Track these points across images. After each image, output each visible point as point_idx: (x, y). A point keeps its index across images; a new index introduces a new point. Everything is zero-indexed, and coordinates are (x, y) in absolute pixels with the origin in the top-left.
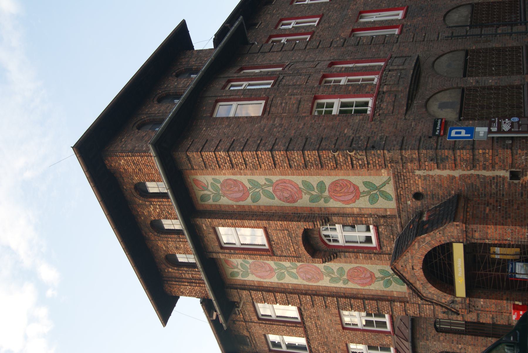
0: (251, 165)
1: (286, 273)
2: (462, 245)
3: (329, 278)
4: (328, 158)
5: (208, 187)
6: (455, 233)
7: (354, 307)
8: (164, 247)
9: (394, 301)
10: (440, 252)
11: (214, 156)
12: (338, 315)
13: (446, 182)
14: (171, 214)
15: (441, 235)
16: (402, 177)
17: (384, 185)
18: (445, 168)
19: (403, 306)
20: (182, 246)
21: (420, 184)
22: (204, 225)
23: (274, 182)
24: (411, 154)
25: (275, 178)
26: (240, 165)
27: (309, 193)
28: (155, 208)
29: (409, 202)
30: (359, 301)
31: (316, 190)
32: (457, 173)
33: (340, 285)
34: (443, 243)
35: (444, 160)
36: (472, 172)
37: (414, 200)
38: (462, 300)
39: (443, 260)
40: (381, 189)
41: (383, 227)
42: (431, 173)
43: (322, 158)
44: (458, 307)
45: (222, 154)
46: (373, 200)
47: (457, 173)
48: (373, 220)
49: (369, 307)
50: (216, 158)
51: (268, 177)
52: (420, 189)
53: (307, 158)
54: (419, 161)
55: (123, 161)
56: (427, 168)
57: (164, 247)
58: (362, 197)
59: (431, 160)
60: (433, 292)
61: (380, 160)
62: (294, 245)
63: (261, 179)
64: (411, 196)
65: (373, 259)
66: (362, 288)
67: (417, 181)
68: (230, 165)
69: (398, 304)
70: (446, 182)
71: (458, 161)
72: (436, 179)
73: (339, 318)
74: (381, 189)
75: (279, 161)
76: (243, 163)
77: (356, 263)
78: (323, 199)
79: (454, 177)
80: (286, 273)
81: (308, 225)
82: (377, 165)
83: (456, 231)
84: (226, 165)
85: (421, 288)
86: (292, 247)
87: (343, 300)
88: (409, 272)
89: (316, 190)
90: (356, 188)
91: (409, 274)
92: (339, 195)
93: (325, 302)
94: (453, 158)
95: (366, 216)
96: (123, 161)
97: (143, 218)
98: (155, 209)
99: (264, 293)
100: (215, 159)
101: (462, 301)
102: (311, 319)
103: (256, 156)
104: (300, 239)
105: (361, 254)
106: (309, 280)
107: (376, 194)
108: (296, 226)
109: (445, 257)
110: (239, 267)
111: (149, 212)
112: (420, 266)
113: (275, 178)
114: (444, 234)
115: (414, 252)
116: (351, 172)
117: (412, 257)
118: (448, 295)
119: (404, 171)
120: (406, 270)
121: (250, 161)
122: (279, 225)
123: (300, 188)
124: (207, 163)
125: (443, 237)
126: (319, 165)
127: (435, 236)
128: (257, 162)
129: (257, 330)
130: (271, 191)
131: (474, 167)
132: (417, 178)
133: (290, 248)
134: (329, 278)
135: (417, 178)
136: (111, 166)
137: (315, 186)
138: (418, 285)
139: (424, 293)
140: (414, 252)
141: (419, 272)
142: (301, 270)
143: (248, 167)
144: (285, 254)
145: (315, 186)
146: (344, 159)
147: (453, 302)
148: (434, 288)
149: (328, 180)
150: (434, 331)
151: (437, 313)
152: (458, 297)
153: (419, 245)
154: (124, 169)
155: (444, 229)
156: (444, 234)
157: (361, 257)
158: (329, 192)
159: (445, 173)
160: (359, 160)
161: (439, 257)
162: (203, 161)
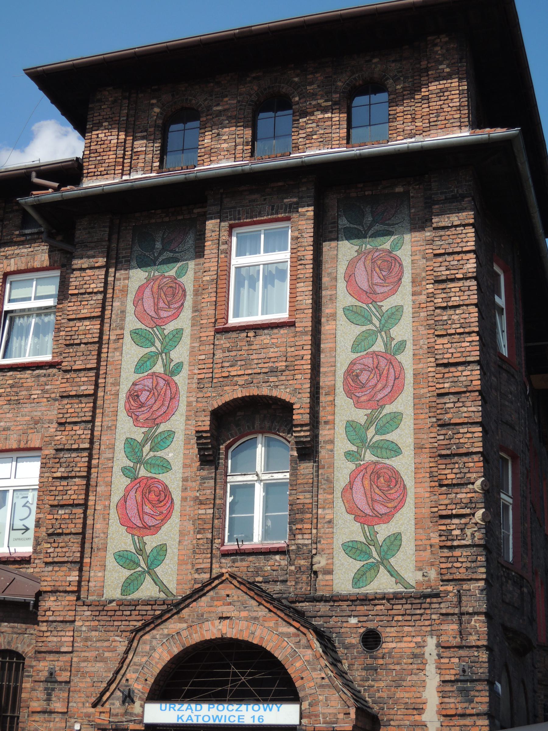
0: (445, 318)
1: (153, 349)
2: (297, 722)
3: (139, 438)
4: (466, 470)
5: (382, 224)
6: (321, 709)
7: (64, 483)
8: (219, 108)
9: (81, 570)
10: (256, 676)
11: (465, 249)
12: (22, 446)
13: (407, 695)
14: (309, 136)
15: (319, 681)
16: (418, 612)
17: (393, 572)
18: (443, 694)
19: (68, 589)
20: (225, 146)
21: (403, 645)
22: (295, 200)
23: (398, 357)
24: (477, 633)
26: (444, 295)
27: (370, 421)
29: (353, 621)
30: (83, 497)
31: (377, 438)
34: (297, 684)
35: (466, 695)
37: (362, 630)
38: (137, 715)
39: (233, 681)
40: (382, 568)
41: (284, 563)
42: (431, 668)
43: (465, 459)
44: (115, 705)
45: (469, 266)
46: (353, 549)
48: (306, 545)
49: (67, 516)
50: (458, 253)
51: (409, 346)
52: (387, 646)
53: (465, 430)
54: (460, 647)
55: (448, 70)
56: (443, 661)
57: (219, 108)
58: (363, 529)
59: (464, 671)
60: (156, 655)
61: (462, 570)
62: (246, 377)
63: (403, 331)
64: (370, 625)
65: (199, 536)
66: (113, 505)
67: (409, 639)
68: (444, 278)
69: (74, 577)
70: (407, 695)
71: (462, 722)
72: (414, 678)
73: (15, 446)
74: (382, 568)
75: (459, 374)
76: (450, 304)
77: (184, 499)
78: (354, 449)
79: (420, 710)
80: (153, 349)
81: (301, 411)
82: (450, 565)
83: (331, 711)
84: (443, 268)
85: (166, 631)
86: (240, 373)
87: (82, 460)
88: (212, 609)
89: (377, 438)
90: (386, 518)
91: (207, 609)
92: (367, 482)
93: (75, 423)
94: (468, 712)
95: (314, 531)
96: (448, 70)
97: (296, 79)
99: (100, 297)
100: (459, 249)
101: (131, 714)
102: (12, 386)
103: (467, 330)
104: (265, 391)
105: (211, 511)
106: (133, 395)
107: (371, 556)
108: (299, 386)
109: (243, 684)
111: (313, 96)
113: (406, 359)
114: (321, 686)
115: (272, 624)
116: (426, 511)
117: (256, 618)
118: (148, 688)
119: (434, 617)
120: (216, 603)
121: (455, 317)
122: (302, 352)
123: (382, 407)
124: (448, 233)
125: (312, 684)
126: (448, 452)
127: (315, 670)
128: (453, 331)
130: (375, 348)
132: (419, 639)
133: (235, 368)
134: (139, 438)
135: (419, 639)
136: (436, 45)
137: (388, 437)
138: (173, 626)
139: (154, 638)
140: (272, 624)
141: (212, 630)
142: (162, 383)
143: (438, 311)
144: (219, 354)
145: (388, 437)
146: (464, 501)
148: (167, 658)
149: (405, 464)
151: (51, 657)
152: (143, 707)
153: (288, 635)
154: (427, 70)
155: (335, 688)
156: (321, 686)
157: (203, 512)
158: (376, 463)
159: (431, 696)
160: (462, 530)
161: (243, 674)
162: (453, 226)
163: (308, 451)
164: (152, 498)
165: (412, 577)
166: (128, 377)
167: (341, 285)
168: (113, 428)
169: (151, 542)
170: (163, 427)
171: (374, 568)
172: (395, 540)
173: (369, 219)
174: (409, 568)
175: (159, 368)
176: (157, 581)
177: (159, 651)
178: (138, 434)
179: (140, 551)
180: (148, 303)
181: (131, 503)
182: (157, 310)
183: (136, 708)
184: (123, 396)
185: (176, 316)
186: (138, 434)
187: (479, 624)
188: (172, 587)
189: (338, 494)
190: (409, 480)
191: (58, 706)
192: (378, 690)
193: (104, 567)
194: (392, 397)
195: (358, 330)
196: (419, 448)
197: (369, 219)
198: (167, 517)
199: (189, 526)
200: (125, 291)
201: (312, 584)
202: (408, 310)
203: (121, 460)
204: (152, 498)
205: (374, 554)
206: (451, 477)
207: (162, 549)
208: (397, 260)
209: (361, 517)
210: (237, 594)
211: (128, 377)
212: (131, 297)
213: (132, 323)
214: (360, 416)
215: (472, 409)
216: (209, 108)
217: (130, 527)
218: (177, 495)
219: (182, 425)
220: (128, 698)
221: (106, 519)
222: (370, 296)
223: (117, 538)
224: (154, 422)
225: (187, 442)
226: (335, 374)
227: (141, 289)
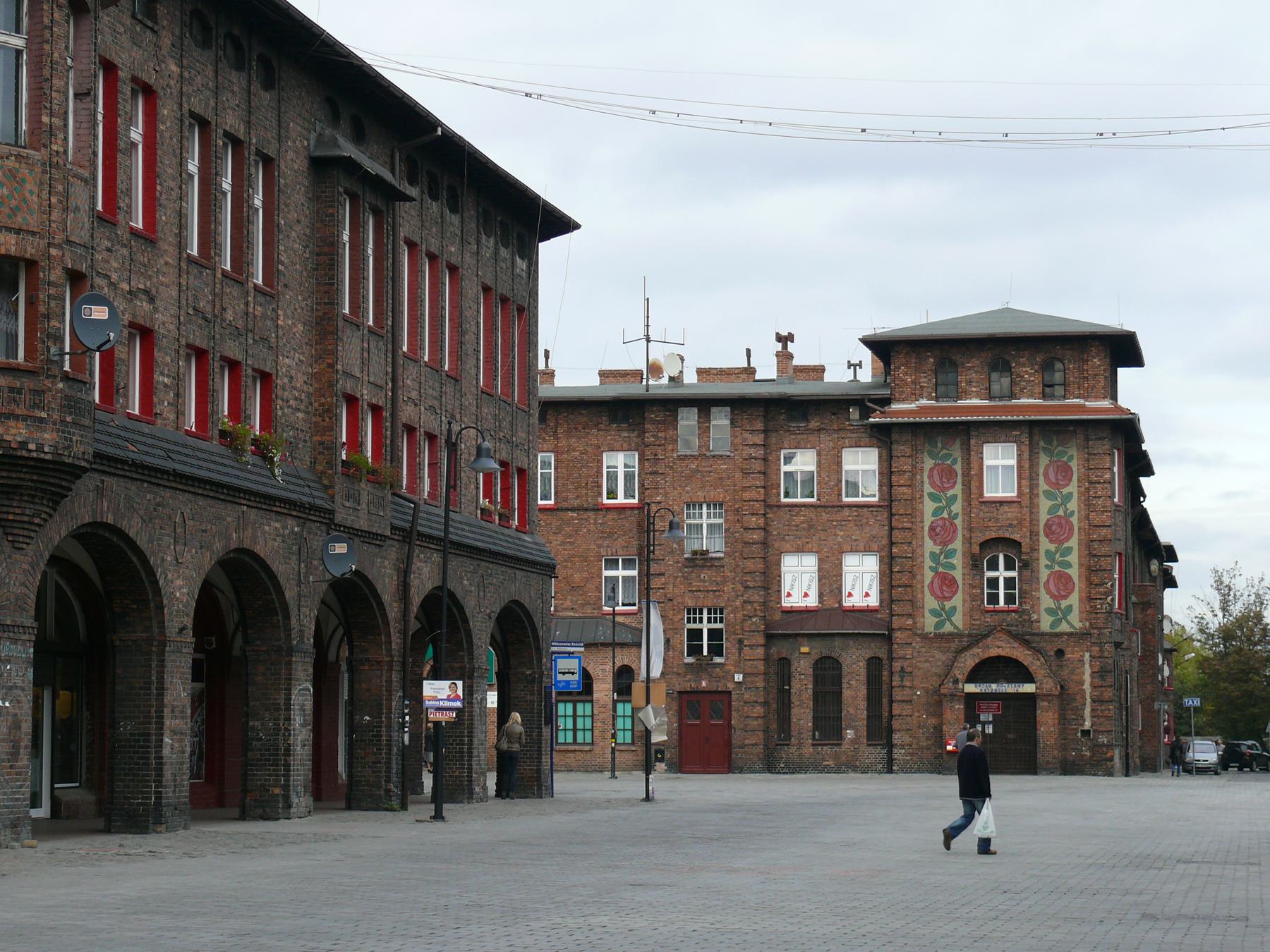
14: (1022, 390)
17: (1069, 623)
25: (1074, 520)
28: (1031, 375)
32: (1087, 687)
33: (928, 563)
35: (1102, 677)
36: (1089, 700)
42: (1087, 666)
46: (1050, 611)
47: (1087, 687)
63: (1073, 505)
90: (1065, 597)
98: (1027, 372)
106: (932, 529)
110: (945, 451)
111: (1024, 365)
112: (1003, 653)
113: (1074, 520)
129: (826, 441)
131: (1093, 701)
138: (976, 650)
141: (994, 652)
147: (956, 681)
149: (1074, 572)
150: (867, 656)
159: (1087, 678)
164: (946, 584)
165: (1078, 625)
166: (928, 519)
167: (1041, 479)
168: (922, 546)
169: (948, 605)
170: (950, 547)
171: (1060, 620)
172: (1070, 608)
173: (1055, 443)
174: (1075, 621)
175: (945, 515)
176: (952, 623)
178: (937, 549)
179: (943, 609)
180: (936, 478)
181: (936, 585)
182: (942, 483)
183: (960, 686)
184: (926, 529)
185: (953, 487)
186: (937, 549)
188: (961, 627)
189: (1042, 585)
190: (1076, 579)
191: (908, 684)
193: (923, 616)
194: (1067, 539)
195: (1051, 503)
196: (1081, 565)
197: (1055, 443)
198: (955, 593)
199: (968, 597)
200: (922, 469)
201: (1030, 627)
202: (1076, 495)
203: (928, 563)
204: (946, 584)
205: (1060, 614)
206: (1096, 580)
207: (954, 608)
208: (1070, 467)
209: (1053, 597)
210: (1004, 637)
211: (928, 519)
212: (926, 474)
213: (928, 488)
214: (1052, 547)
216: (963, 364)
217: (937, 597)
218: (960, 582)
220: (956, 681)
221: (923, 592)
222: (1057, 486)
223: (930, 602)
224: (944, 543)
225: (964, 555)
227: (931, 470)
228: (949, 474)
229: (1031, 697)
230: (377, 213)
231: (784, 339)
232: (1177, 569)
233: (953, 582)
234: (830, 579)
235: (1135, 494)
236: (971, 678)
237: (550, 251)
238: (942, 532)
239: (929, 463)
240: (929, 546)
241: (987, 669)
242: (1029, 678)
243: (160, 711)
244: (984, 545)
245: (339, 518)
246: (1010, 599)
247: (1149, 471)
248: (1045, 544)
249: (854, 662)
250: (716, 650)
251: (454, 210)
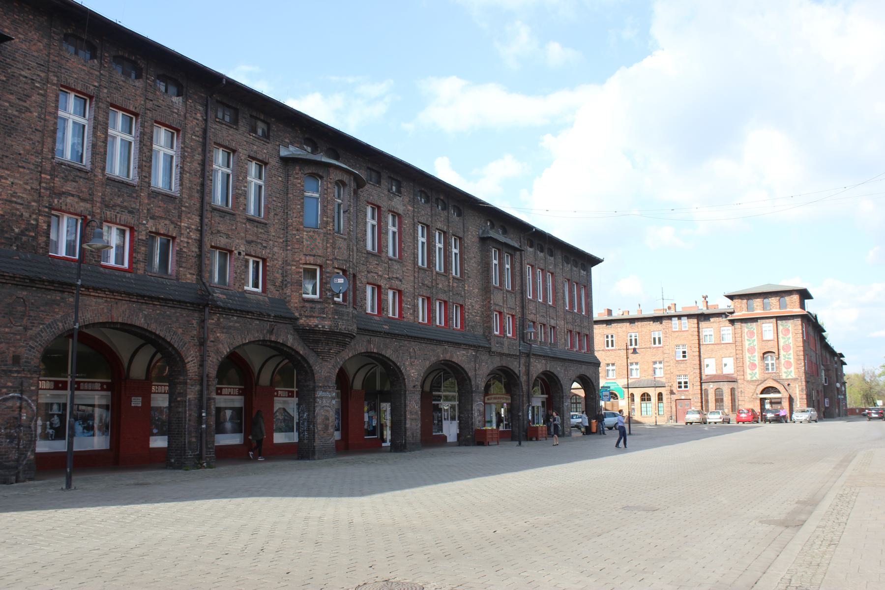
33: (748, 359)
129: (716, 325)
149: (792, 361)
159: (798, 392)
163: (778, 358)
174: (793, 375)
177: (761, 388)
187: (804, 383)
192: (790, 391)
203: (748, 359)
204: (753, 365)
213: (746, 338)
215: (802, 353)
219: (757, 356)
223: (748, 371)
226: (781, 348)
228: (753, 333)
229: (780, 398)
230: (511, 255)
231: (705, 297)
232: (844, 360)
233: (755, 365)
234: (720, 365)
235: (823, 339)
236: (762, 393)
237: (595, 270)
238: (752, 350)
239: (746, 330)
240: (747, 355)
241: (766, 390)
242: (779, 392)
243: (405, 413)
244: (764, 354)
245: (493, 350)
246: (773, 369)
247: (824, 331)
248: (782, 353)
249: (726, 388)
250: (686, 387)
251: (551, 255)
